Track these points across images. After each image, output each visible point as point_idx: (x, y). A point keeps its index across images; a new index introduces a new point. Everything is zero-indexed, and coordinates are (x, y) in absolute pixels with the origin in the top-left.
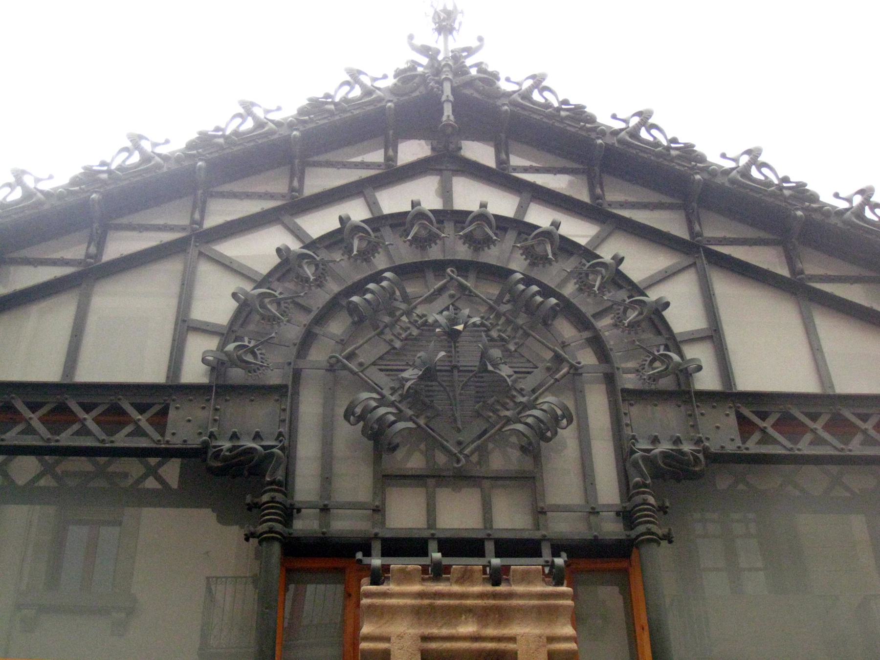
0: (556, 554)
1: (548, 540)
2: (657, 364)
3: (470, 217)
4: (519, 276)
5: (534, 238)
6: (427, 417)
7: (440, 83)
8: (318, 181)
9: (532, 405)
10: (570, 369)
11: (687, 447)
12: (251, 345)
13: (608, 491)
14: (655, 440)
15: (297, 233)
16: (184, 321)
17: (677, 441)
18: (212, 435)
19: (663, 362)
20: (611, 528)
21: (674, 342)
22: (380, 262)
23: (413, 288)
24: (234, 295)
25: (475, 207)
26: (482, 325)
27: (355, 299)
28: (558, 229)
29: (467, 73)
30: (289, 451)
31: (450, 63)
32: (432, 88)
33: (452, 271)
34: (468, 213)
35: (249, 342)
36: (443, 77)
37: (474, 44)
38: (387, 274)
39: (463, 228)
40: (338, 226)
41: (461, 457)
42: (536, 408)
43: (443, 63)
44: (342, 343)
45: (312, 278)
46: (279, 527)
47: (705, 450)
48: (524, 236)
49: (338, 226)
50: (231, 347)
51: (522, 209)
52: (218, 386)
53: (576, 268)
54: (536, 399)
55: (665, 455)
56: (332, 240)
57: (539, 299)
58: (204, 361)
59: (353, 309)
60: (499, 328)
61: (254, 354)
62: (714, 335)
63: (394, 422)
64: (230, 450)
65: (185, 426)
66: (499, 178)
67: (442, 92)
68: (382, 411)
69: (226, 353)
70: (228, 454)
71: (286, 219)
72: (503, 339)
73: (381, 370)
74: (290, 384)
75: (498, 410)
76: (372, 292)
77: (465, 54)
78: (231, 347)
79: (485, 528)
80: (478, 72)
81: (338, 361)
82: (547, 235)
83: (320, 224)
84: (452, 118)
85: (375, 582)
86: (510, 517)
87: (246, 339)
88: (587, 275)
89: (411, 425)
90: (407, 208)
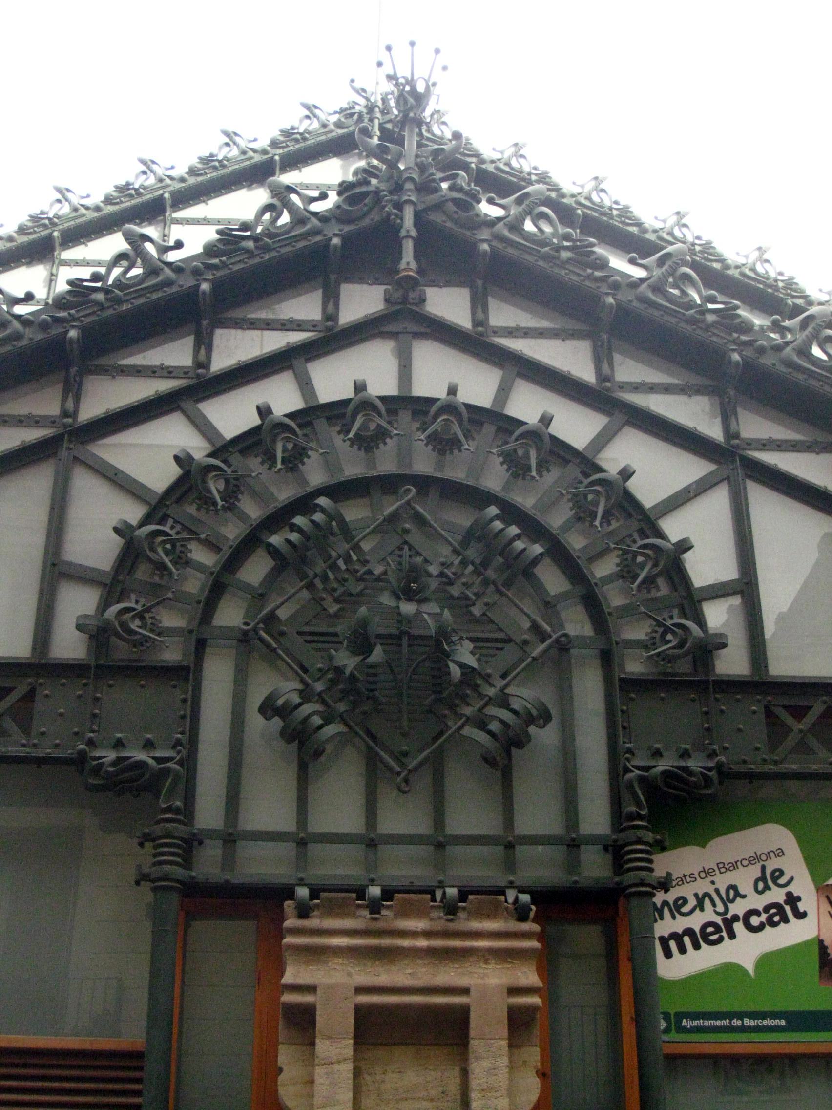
2: (669, 637)
3: (434, 409)
5: (517, 440)
7: (399, 206)
8: (233, 348)
11: (695, 764)
13: (596, 818)
14: (657, 754)
15: (204, 428)
16: (54, 565)
18: (91, 743)
19: (674, 633)
20: (595, 868)
21: (691, 600)
23: (354, 512)
25: (439, 392)
28: (547, 428)
29: (437, 190)
30: (190, 762)
31: (415, 176)
32: (389, 214)
34: (431, 401)
36: (405, 198)
43: (406, 175)
44: (259, 597)
49: (257, 421)
51: (503, 392)
52: (98, 667)
56: (250, 442)
58: (80, 627)
59: (273, 552)
60: (464, 580)
62: (746, 588)
63: (320, 727)
64: (114, 763)
65: (56, 722)
66: (475, 344)
67: (402, 219)
68: (307, 709)
70: (110, 769)
71: (187, 405)
72: (467, 598)
74: (192, 666)
80: (451, 188)
83: (232, 415)
84: (413, 265)
90: (347, 393)
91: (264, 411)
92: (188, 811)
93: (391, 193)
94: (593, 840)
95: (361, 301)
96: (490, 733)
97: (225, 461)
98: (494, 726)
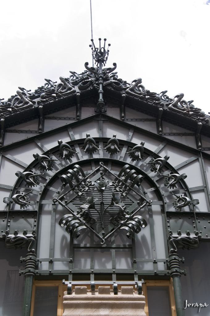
0: (140, 280)
1: (137, 274)
4: (127, 166)
6: (91, 223)
7: (98, 84)
9: (131, 219)
10: (147, 203)
12: (23, 195)
17: (188, 234)
21: (188, 192)
22: (74, 160)
24: (17, 174)
26: (113, 185)
27: (64, 176)
33: (101, 163)
35: (22, 194)
37: (113, 67)
38: (77, 166)
39: (107, 145)
40: (58, 145)
41: (104, 240)
42: (133, 220)
45: (47, 167)
46: (32, 270)
47: (199, 237)
48: (130, 148)
50: (15, 196)
53: (150, 161)
54: (133, 216)
55: (183, 240)
56: (56, 151)
57: (135, 175)
61: (24, 199)
63: (78, 226)
66: (122, 125)
69: (13, 199)
72: (121, 191)
73: (73, 204)
75: (119, 220)
76: (70, 173)
77: (108, 71)
78: (15, 196)
79: (113, 269)
81: (57, 201)
82: (139, 149)
84: (102, 100)
85: (69, 293)
86: (123, 265)
87: (21, 192)
88: (154, 164)
89: (85, 227)
91: (60, 143)
92: (35, 254)
93: (96, 81)
94: (161, 261)
95: (87, 113)
96: (129, 227)
97: (48, 156)
98: (130, 225)
